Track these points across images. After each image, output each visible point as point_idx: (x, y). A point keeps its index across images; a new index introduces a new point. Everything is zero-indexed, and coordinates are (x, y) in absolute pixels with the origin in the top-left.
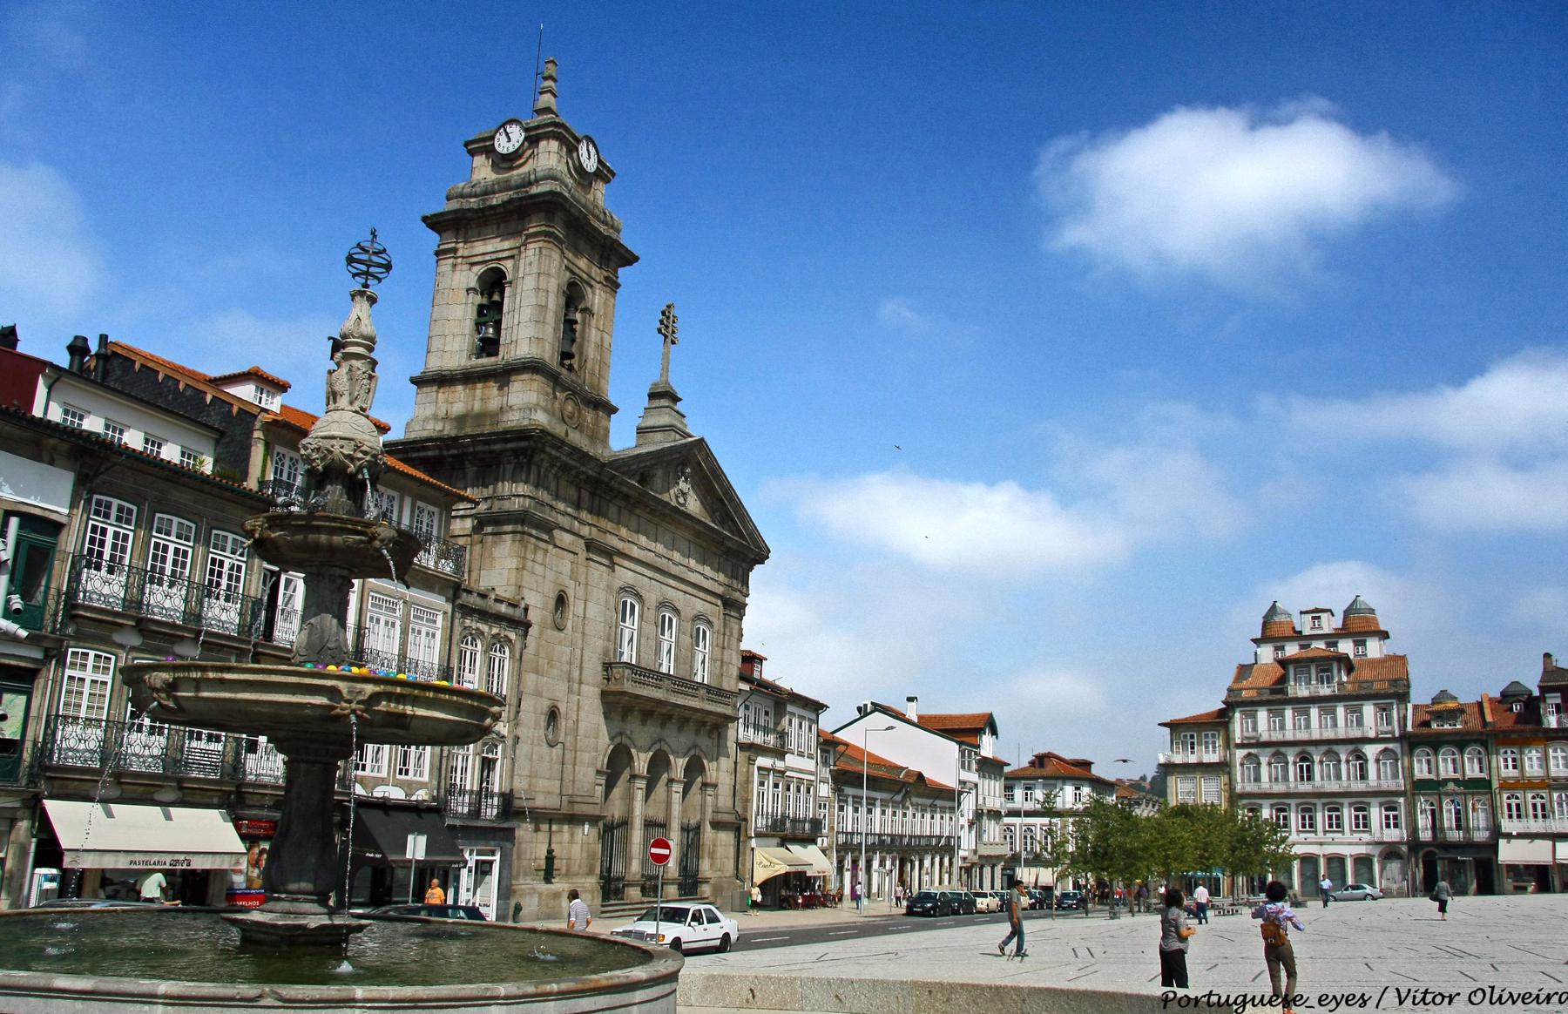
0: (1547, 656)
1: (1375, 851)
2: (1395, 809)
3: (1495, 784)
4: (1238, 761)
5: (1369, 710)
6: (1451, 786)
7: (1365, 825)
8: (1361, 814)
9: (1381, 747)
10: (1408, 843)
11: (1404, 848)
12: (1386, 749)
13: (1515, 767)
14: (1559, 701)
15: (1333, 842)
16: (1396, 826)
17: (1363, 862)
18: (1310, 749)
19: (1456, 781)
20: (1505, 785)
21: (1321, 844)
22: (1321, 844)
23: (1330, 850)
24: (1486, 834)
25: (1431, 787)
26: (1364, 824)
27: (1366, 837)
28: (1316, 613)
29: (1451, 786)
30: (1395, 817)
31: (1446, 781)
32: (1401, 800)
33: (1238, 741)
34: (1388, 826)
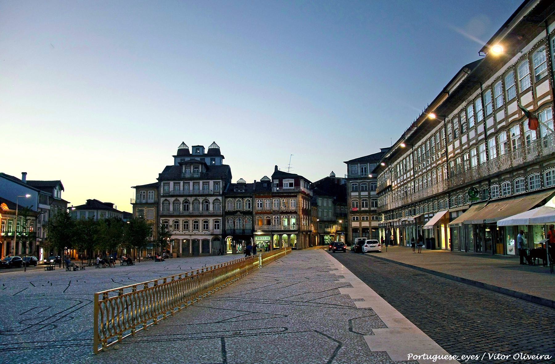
0: (276, 167)
1: (210, 238)
2: (218, 222)
3: (254, 213)
4: (161, 202)
6: (239, 213)
7: (207, 228)
8: (206, 224)
9: (214, 198)
10: (221, 235)
11: (221, 237)
12: (217, 199)
13: (261, 206)
14: (278, 182)
15: (195, 235)
16: (218, 228)
17: (205, 242)
18: (189, 198)
19: (239, 211)
20: (257, 213)
21: (191, 235)
22: (191, 235)
23: (193, 237)
24: (250, 231)
25: (233, 213)
26: (206, 227)
27: (207, 232)
29: (239, 213)
30: (218, 225)
31: (237, 211)
32: (221, 218)
34: (215, 228)
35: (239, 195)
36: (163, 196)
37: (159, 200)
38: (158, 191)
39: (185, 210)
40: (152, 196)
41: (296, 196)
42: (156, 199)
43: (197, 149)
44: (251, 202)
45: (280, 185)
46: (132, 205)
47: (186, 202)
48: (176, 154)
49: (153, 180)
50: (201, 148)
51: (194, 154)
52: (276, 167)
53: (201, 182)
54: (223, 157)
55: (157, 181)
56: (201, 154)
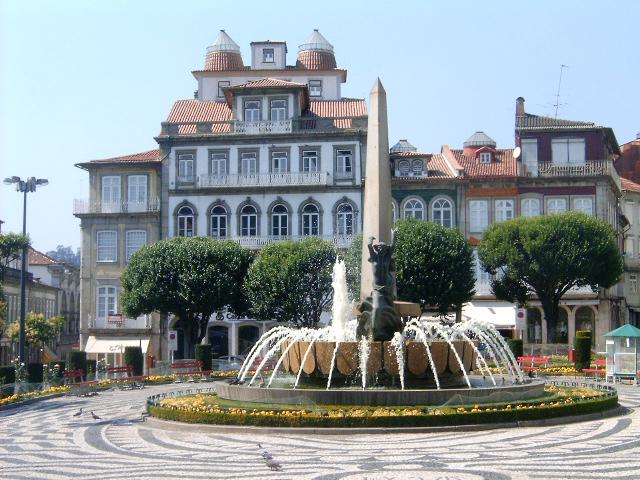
5: (327, 149)
9: (339, 196)
18: (256, 198)
28: (267, 48)
33: (172, 187)
35: (413, 188)
36: (178, 192)
37: (164, 203)
38: (160, 176)
39: (276, 232)
40: (140, 196)
41: (590, 191)
42: (155, 201)
43: (265, 52)
44: (451, 209)
45: (545, 155)
46: (79, 221)
47: (218, 209)
48: (202, 68)
49: (144, 143)
50: (278, 51)
51: (259, 66)
52: (521, 100)
53: (295, 148)
54: (343, 76)
55: (157, 146)
56: (279, 66)
